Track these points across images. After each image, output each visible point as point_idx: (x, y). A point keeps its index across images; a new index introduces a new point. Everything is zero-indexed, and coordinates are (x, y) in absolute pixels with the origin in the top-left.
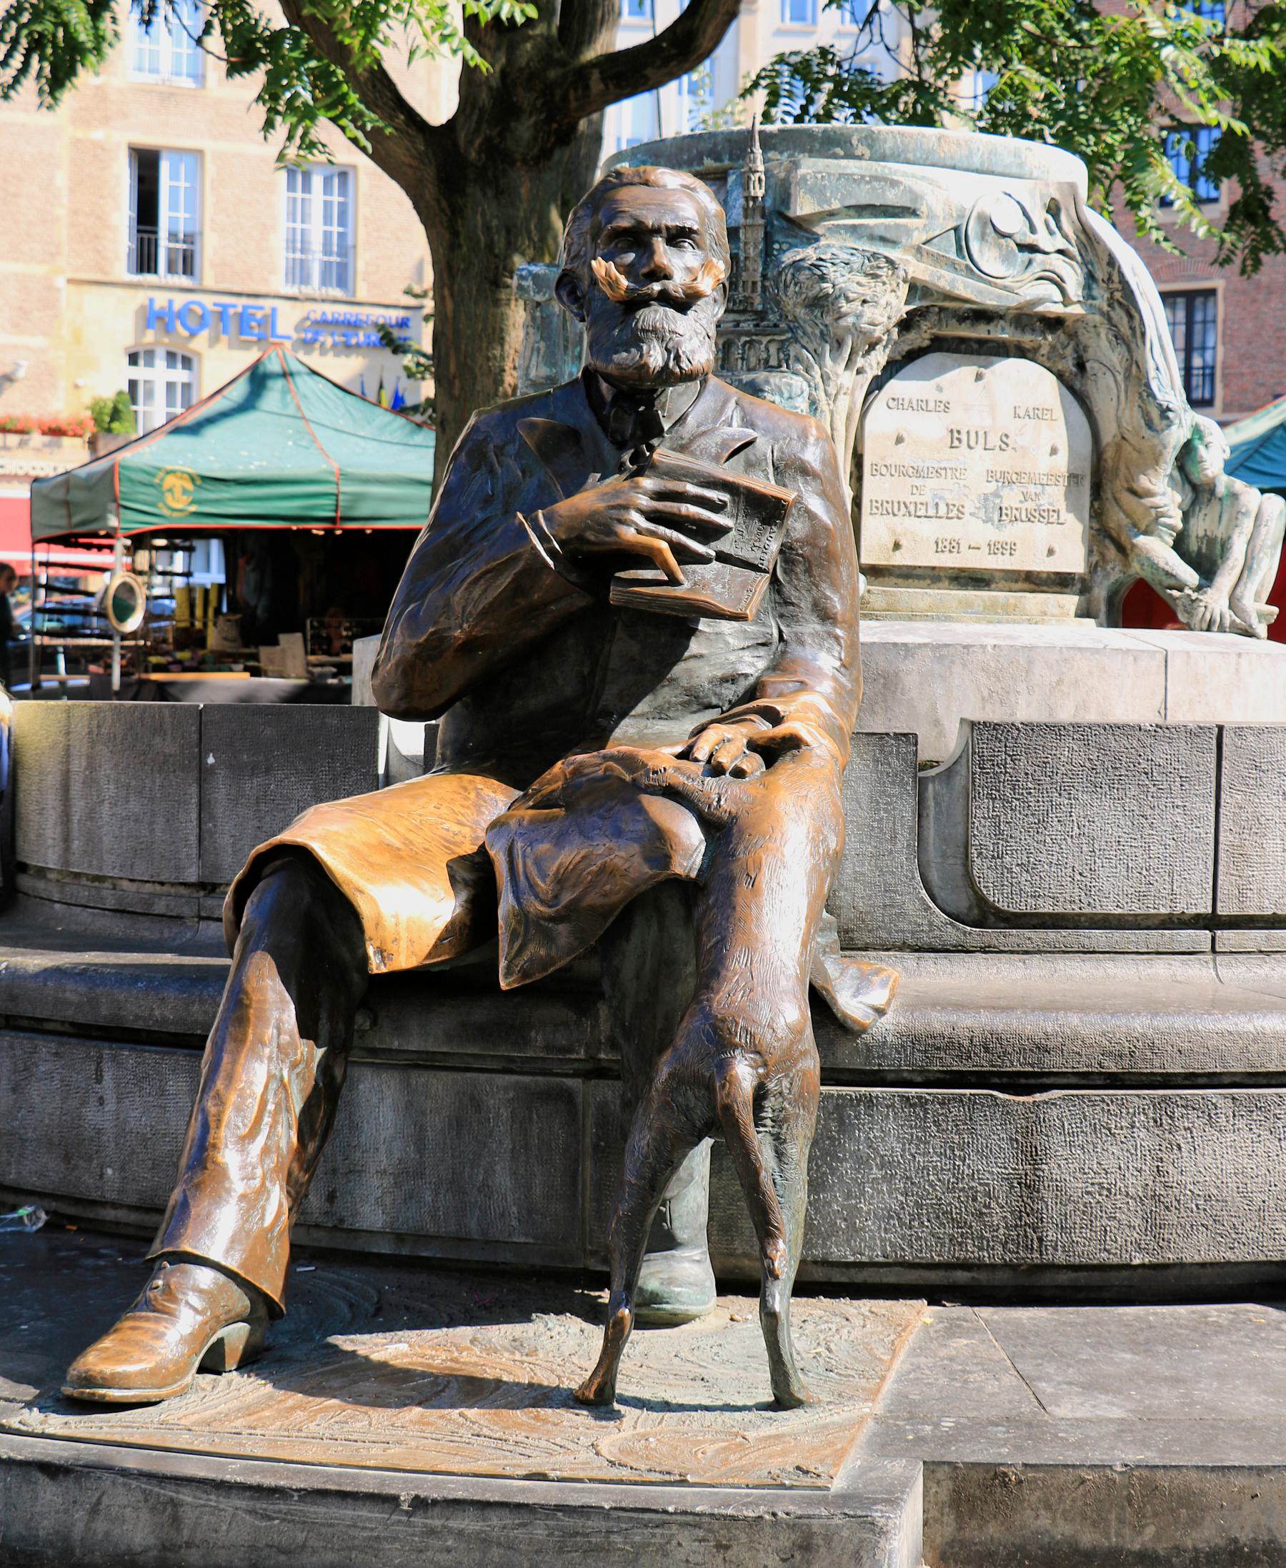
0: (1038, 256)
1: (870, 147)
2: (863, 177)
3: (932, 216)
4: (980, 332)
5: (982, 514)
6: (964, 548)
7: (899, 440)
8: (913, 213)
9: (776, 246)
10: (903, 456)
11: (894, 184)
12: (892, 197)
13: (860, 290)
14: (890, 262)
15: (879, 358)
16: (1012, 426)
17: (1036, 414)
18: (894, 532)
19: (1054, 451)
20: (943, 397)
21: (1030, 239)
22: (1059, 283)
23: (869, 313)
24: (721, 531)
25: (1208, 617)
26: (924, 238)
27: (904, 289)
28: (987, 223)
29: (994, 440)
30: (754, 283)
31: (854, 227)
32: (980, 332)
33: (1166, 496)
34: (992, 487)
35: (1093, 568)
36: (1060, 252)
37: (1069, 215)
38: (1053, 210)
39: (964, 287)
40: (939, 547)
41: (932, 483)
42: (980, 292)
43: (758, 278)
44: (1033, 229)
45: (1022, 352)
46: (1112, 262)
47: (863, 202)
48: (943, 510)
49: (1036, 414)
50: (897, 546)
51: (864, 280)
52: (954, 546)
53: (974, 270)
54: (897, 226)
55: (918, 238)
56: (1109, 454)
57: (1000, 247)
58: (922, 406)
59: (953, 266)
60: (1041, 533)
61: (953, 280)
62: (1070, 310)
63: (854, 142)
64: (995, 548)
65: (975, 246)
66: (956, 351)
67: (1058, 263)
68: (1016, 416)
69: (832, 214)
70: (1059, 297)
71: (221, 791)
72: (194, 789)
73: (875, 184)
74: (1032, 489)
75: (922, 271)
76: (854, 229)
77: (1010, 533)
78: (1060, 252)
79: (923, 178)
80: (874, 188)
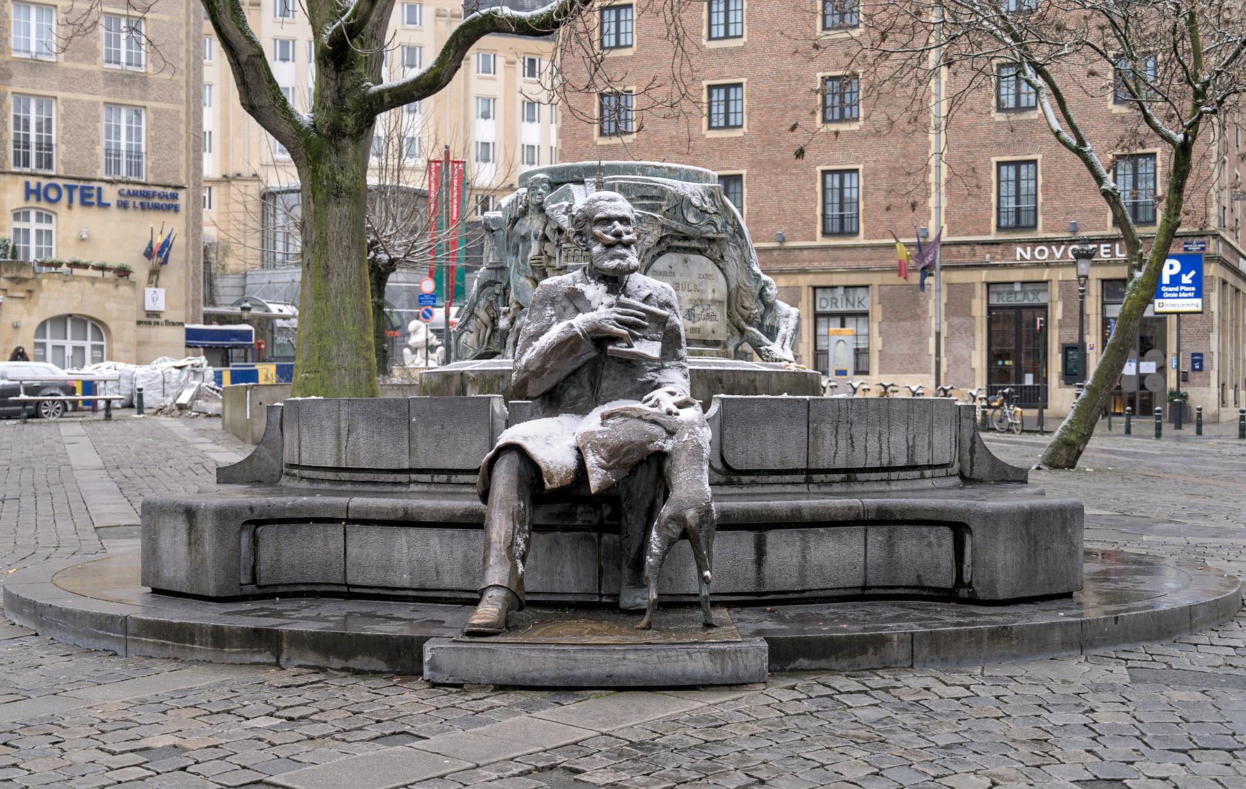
4: (686, 244)
8: (663, 199)
11: (656, 187)
12: (654, 192)
15: (650, 255)
16: (698, 281)
17: (707, 276)
22: (715, 225)
24: (644, 327)
29: (692, 287)
32: (686, 244)
33: (757, 310)
35: (728, 338)
39: (681, 227)
45: (700, 252)
46: (734, 217)
49: (707, 276)
55: (664, 208)
56: (734, 292)
60: (709, 325)
67: (714, 218)
71: (419, 432)
72: (406, 432)
75: (665, 221)
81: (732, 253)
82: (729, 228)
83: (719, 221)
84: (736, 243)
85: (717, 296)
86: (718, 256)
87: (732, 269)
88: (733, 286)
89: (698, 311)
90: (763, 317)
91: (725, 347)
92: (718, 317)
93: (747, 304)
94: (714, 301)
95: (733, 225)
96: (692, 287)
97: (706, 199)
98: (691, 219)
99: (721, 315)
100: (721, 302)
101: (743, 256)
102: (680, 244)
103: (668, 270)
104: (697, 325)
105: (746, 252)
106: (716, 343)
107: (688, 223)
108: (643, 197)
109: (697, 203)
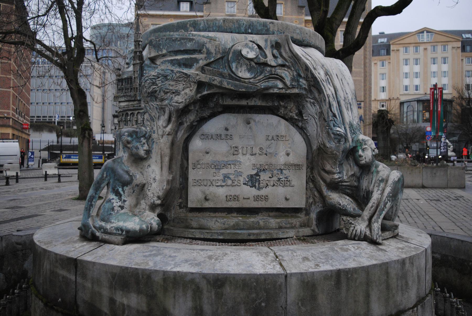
0: (268, 69)
1: (194, 27)
2: (177, 38)
3: (209, 53)
6: (241, 199)
7: (207, 153)
8: (200, 52)
9: (145, 72)
10: (208, 159)
11: (191, 40)
12: (189, 46)
13: (171, 88)
14: (186, 74)
15: (191, 118)
16: (265, 144)
17: (278, 138)
18: (204, 193)
19: (288, 155)
20: (229, 133)
21: (262, 60)
22: (281, 79)
23: (176, 98)
25: (354, 232)
26: (205, 62)
27: (194, 87)
28: (239, 55)
29: (256, 150)
30: (137, 88)
31: (172, 61)
34: (254, 172)
36: (283, 66)
37: (285, 50)
38: (277, 46)
40: (229, 198)
41: (224, 171)
42: (236, 86)
43: (138, 86)
44: (266, 56)
45: (273, 111)
47: (176, 49)
48: (229, 182)
49: (278, 138)
50: (206, 199)
51: (172, 83)
52: (236, 198)
53: (234, 77)
54: (191, 58)
55: (201, 63)
57: (247, 65)
58: (219, 137)
59: (221, 75)
60: (281, 191)
61: (221, 82)
62: (288, 91)
63: (188, 26)
64: (257, 198)
65: (234, 65)
66: (238, 112)
67: (280, 71)
68: (267, 139)
69: (164, 56)
70: (280, 85)
73: (182, 41)
74: (275, 172)
75: (204, 78)
76: (172, 62)
77: (263, 192)
78: (283, 66)
79: (203, 36)
80: (182, 43)
81: (311, 110)
82: (303, 82)
83: (287, 75)
84: (314, 98)
85: (292, 159)
86: (294, 115)
87: (313, 127)
88: (315, 147)
89: (264, 177)
90: (359, 179)
91: (308, 214)
92: (293, 183)
93: (328, 167)
94: (289, 166)
95: (306, 79)
96: (256, 150)
97: (268, 52)
98: (244, 73)
99: (299, 180)
100: (297, 167)
101: (321, 113)
102: (235, 102)
104: (263, 192)
105: (325, 108)
107: (239, 79)
108: (177, 52)
109: (251, 55)
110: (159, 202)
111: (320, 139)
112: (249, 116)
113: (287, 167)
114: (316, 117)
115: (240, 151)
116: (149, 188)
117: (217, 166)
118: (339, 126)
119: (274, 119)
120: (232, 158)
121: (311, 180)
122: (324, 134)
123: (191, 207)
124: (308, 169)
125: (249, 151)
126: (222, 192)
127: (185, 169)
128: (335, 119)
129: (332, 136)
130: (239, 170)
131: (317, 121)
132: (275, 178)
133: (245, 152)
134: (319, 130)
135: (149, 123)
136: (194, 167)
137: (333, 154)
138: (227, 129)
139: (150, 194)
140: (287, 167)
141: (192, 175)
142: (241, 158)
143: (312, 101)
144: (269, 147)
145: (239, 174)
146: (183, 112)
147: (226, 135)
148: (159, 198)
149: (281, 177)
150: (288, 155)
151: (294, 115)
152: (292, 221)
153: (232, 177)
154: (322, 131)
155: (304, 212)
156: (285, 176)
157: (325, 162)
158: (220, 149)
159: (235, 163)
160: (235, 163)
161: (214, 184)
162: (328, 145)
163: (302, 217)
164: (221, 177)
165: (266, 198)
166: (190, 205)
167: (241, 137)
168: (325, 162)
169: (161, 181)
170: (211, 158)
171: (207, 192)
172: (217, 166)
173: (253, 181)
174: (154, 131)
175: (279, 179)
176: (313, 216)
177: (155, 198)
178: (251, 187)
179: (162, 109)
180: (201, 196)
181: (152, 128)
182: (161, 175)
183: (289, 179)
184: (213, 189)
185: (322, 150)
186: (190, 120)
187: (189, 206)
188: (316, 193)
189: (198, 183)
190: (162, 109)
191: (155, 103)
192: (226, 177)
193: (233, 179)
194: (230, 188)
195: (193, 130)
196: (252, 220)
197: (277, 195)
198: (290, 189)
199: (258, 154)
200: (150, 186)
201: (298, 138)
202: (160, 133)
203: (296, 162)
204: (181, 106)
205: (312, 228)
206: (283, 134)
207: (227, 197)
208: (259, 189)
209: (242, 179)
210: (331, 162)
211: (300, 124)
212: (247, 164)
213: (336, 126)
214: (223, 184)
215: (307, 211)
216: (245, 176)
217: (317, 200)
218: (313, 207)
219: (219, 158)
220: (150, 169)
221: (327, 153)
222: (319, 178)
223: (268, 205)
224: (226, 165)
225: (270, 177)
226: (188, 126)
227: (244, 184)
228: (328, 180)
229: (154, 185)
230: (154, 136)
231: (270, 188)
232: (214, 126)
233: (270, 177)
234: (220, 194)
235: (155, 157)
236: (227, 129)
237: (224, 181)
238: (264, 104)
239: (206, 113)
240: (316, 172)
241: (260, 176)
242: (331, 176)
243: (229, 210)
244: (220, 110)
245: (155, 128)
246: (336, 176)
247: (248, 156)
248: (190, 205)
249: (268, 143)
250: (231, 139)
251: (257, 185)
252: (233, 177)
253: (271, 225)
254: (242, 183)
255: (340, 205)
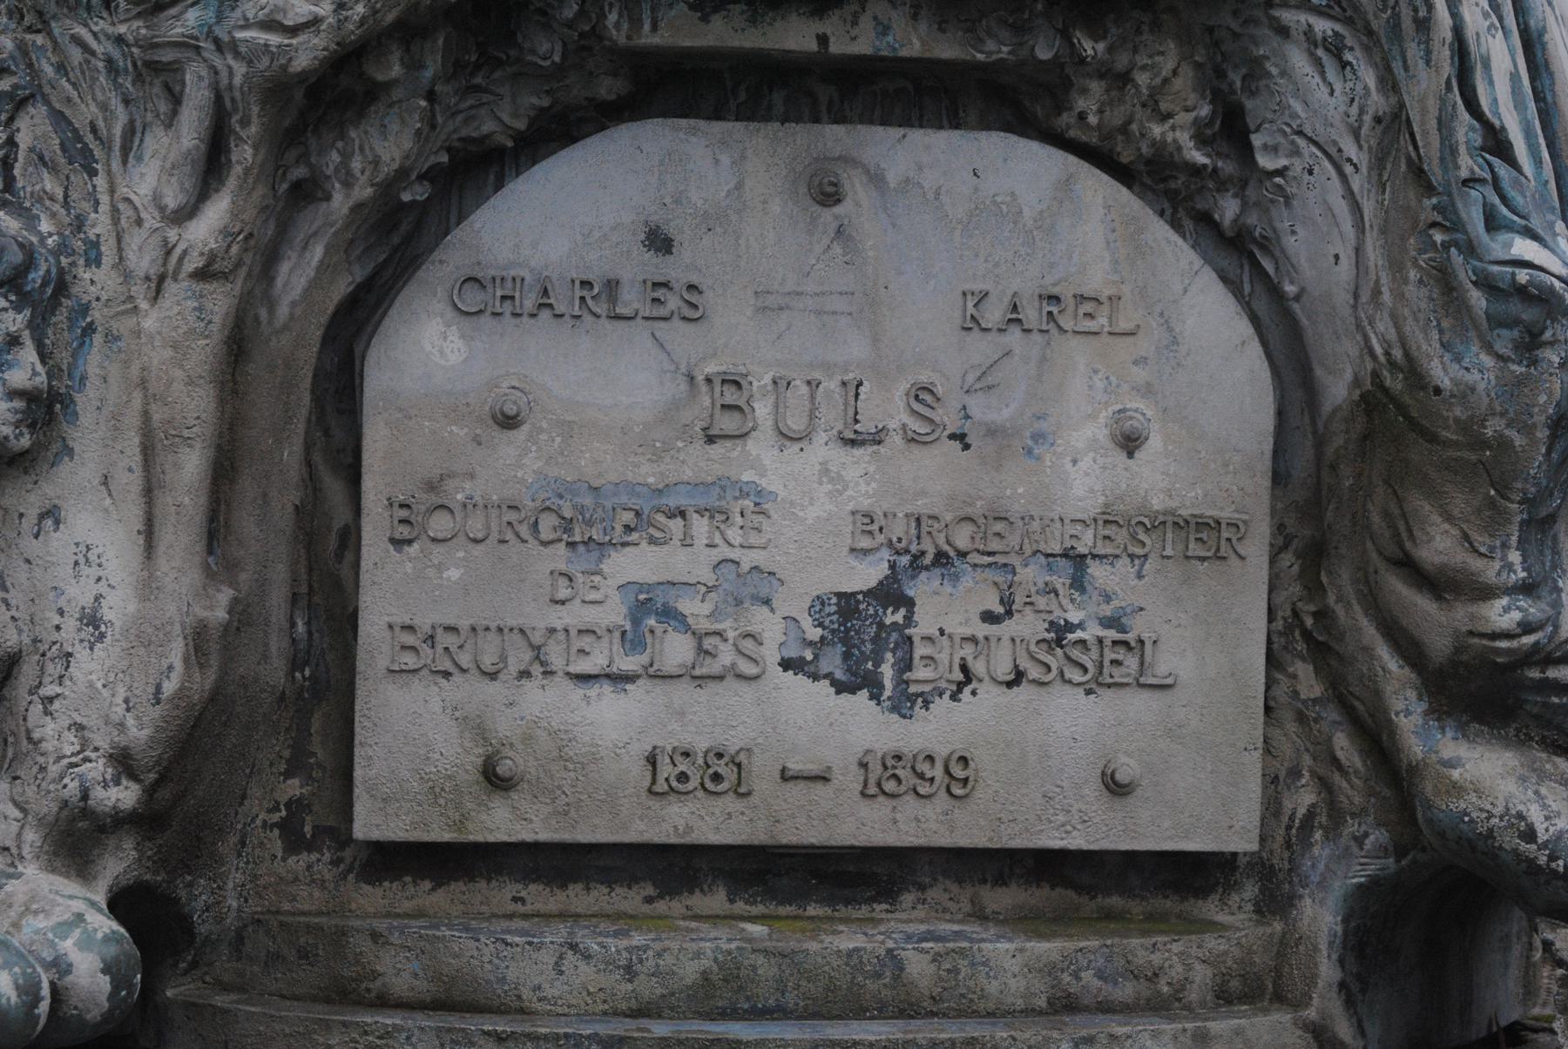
5: (832, 661)
7: (508, 422)
10: (516, 465)
16: (950, 359)
18: (478, 729)
19: (1130, 443)
20: (674, 269)
29: (886, 407)
34: (867, 575)
35: (1286, 837)
40: (666, 773)
41: (635, 564)
50: (495, 779)
52: (723, 772)
58: (598, 297)
60: (1071, 720)
64: (887, 776)
66: (752, 112)
68: (973, 324)
74: (1031, 575)
85: (1156, 479)
86: (1180, 134)
87: (1327, 235)
88: (1337, 390)
89: (944, 610)
91: (1276, 899)
92: (1164, 664)
93: (1439, 545)
96: (886, 407)
99: (1211, 643)
100: (1201, 536)
101: (1395, 123)
103: (636, 266)
104: (936, 729)
105: (1427, 83)
106: (1188, 876)
110: (125, 795)
111: (1384, 325)
112: (834, 137)
113: (1121, 536)
114: (1350, 150)
115: (762, 410)
116: (49, 690)
117: (583, 526)
118: (1536, 223)
119: (1022, 168)
120: (698, 462)
121: (1302, 635)
122: (1411, 290)
123: (376, 835)
124: (1287, 559)
125: (832, 417)
126: (616, 723)
127: (333, 542)
128: (1503, 170)
129: (1478, 300)
130: (748, 559)
131: (1356, 183)
132: (1027, 626)
133: (796, 423)
134: (1374, 255)
135: (50, 184)
136: (404, 532)
137: (1481, 443)
138: (659, 242)
139: (52, 732)
140: (1121, 536)
141: (394, 591)
142: (764, 461)
143: (1322, 26)
144: (985, 381)
145: (751, 587)
146: (322, 99)
147: (651, 287)
148: (124, 762)
149: (1074, 616)
150: (1130, 443)
151: (1180, 134)
152: (1156, 958)
153: (693, 607)
154: (1396, 267)
155: (1250, 890)
156: (1107, 610)
157: (1421, 505)
158: (609, 385)
159: (721, 502)
160: (721, 502)
161: (557, 660)
162: (1441, 372)
163: (1234, 926)
164: (614, 613)
165: (957, 776)
166: (369, 823)
167: (768, 305)
168: (1421, 505)
169: (144, 638)
170: (533, 463)
171: (504, 726)
172: (583, 526)
173: (861, 640)
174: (96, 245)
175: (1059, 633)
176: (1321, 916)
177: (97, 769)
178: (841, 688)
179: (157, 74)
180: (454, 755)
181: (79, 224)
182: (148, 587)
183: (1138, 627)
184: (547, 702)
185: (1394, 412)
186: (376, 162)
187: (360, 831)
188: (1343, 744)
189: (436, 651)
190: (157, 74)
191: (100, 25)
192: (651, 608)
193: (705, 625)
194: (683, 693)
195: (397, 244)
196: (845, 940)
197: (1044, 754)
198: (1141, 705)
199: (896, 440)
200: (53, 669)
201: (1210, 315)
202: (143, 261)
203: (1190, 502)
204: (306, 54)
205: (1311, 1013)
206: (1097, 280)
207: (652, 760)
208: (906, 702)
209: (770, 626)
210: (1460, 502)
211: (1228, 209)
212: (813, 512)
213: (1510, 228)
214: (628, 664)
215: (1270, 880)
216: (794, 601)
217: (1351, 793)
218: (1320, 851)
219: (600, 461)
220: (59, 543)
221: (1433, 439)
222: (1370, 632)
223: (967, 828)
224: (649, 517)
225: (989, 617)
226: (357, 208)
227: (786, 664)
228: (1439, 645)
229: (89, 666)
230: (97, 283)
231: (986, 701)
232: (565, 209)
233: (989, 617)
234: (603, 743)
235: (97, 445)
236: (659, 242)
237: (633, 640)
238: (948, 49)
239: (502, 117)
240: (1341, 581)
241: (910, 603)
242: (1460, 615)
243: (673, 868)
244: (608, 88)
245: (100, 225)
246: (1502, 614)
247: (822, 450)
248: (369, 823)
249: (981, 348)
250: (693, 314)
251: (887, 671)
252: (706, 608)
253: (993, 987)
254: (771, 656)
255: (1530, 835)
